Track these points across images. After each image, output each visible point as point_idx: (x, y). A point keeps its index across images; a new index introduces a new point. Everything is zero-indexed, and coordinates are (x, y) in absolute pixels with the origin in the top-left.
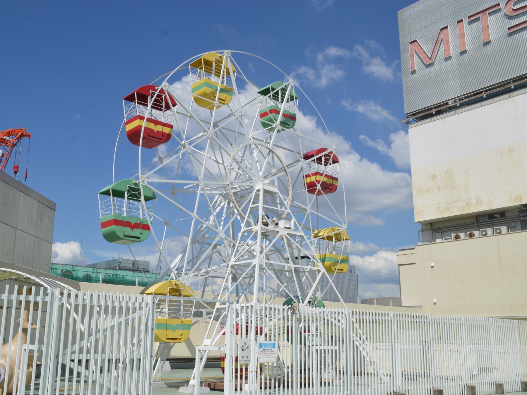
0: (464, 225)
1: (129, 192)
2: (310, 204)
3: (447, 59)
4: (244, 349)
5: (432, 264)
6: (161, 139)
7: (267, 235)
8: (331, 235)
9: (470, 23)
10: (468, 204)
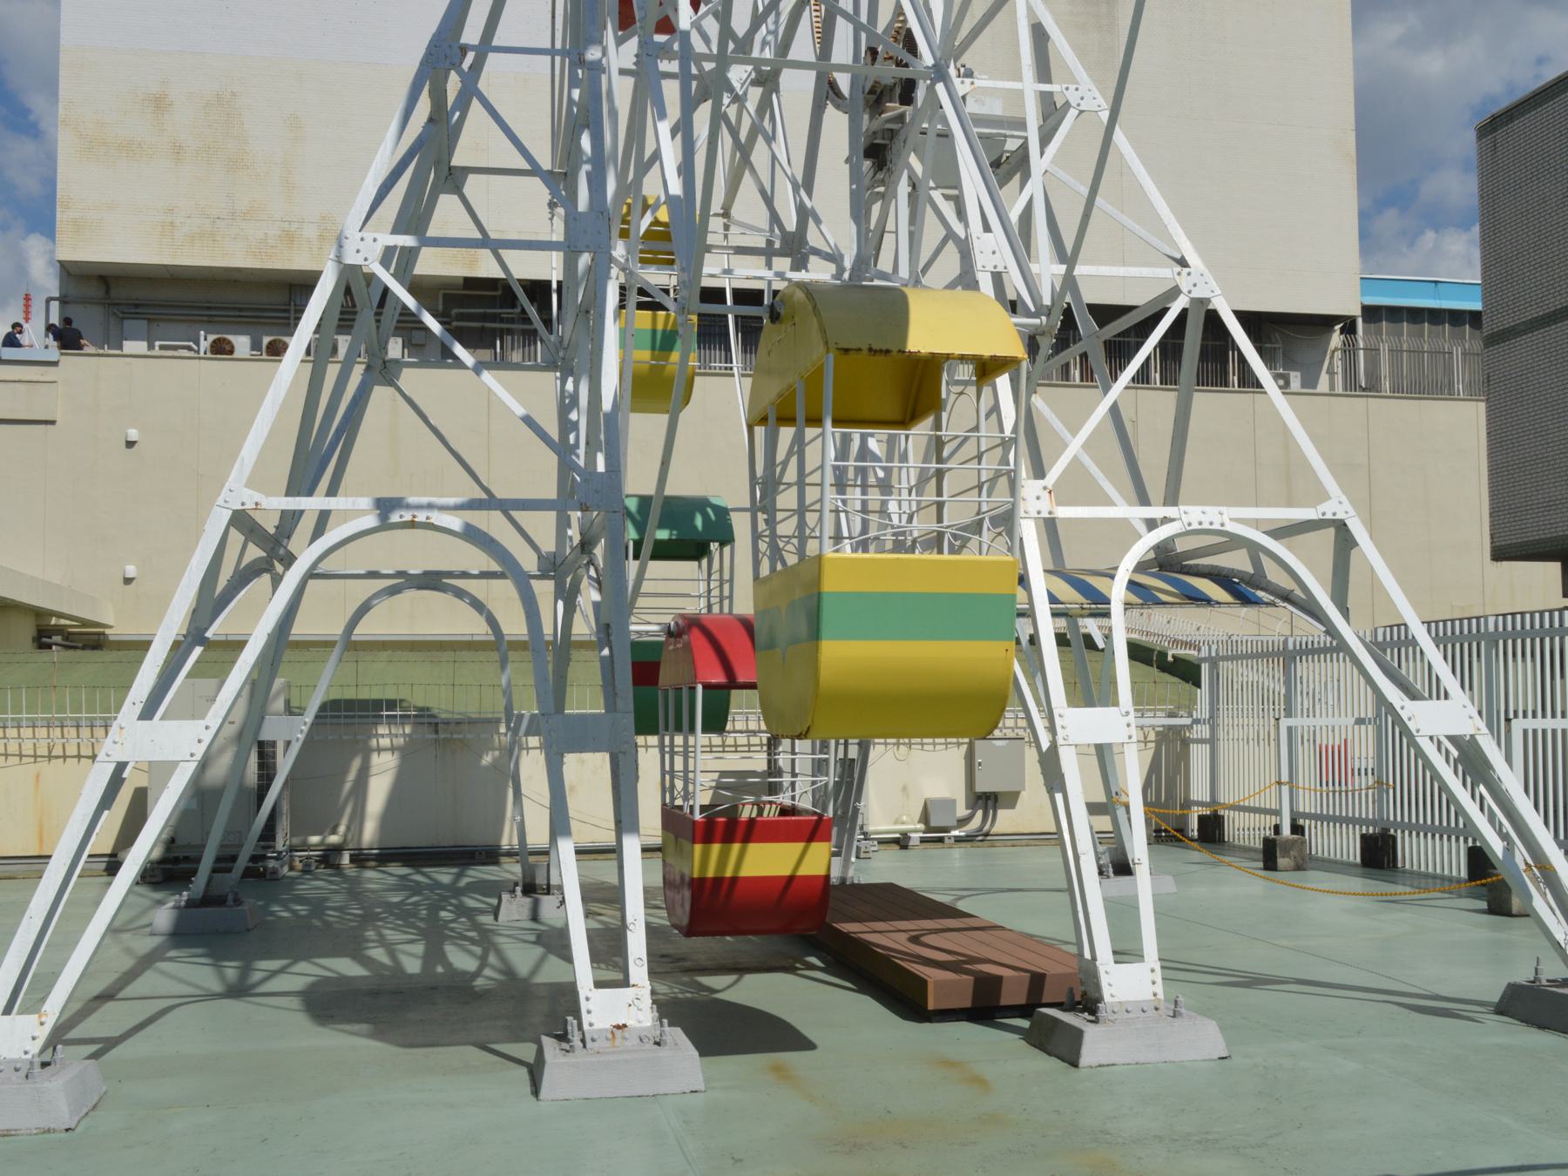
0: (241, 310)
5: (133, 434)
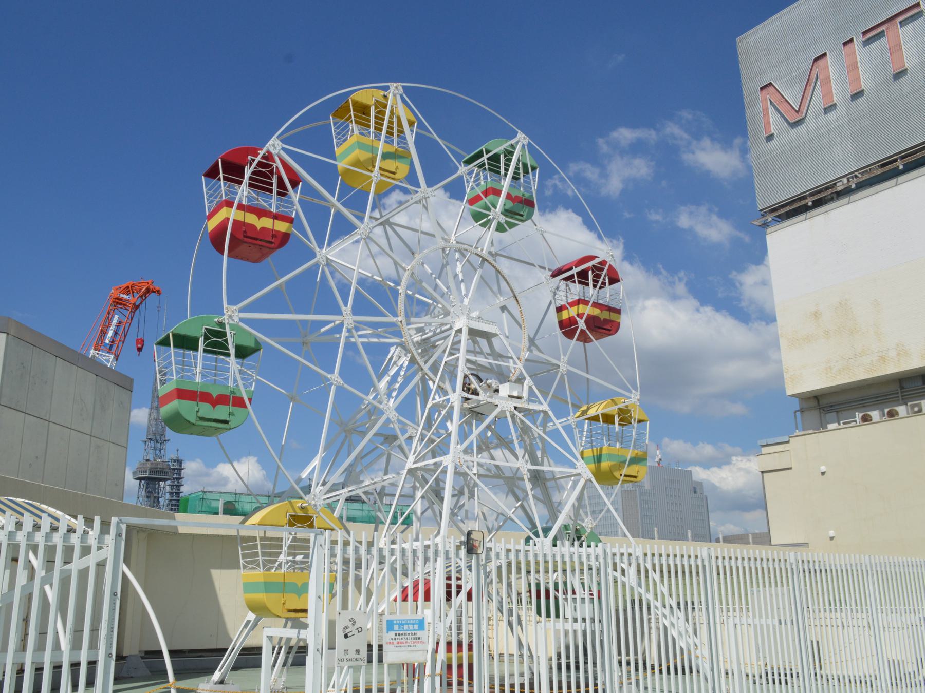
1: (206, 338)
2: (565, 355)
3: (827, 110)
4: (349, 635)
5: (823, 469)
6: (272, 243)
7: (479, 413)
8: (610, 413)
9: (867, 43)
10: (883, 359)
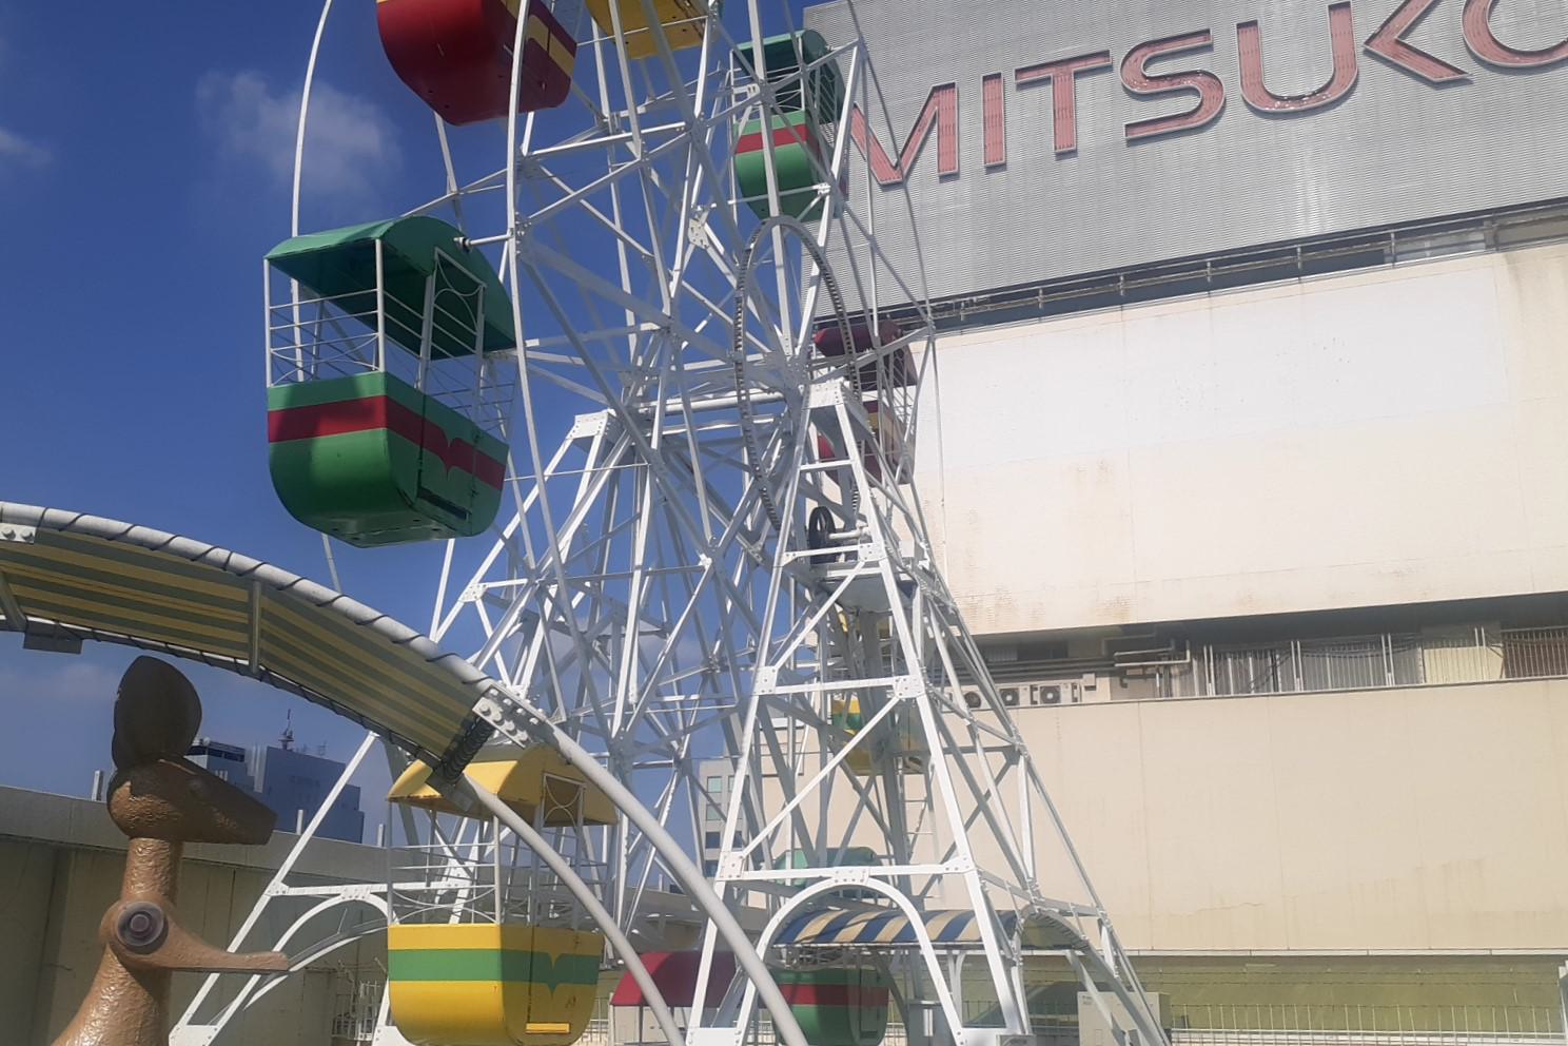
9: (1021, 86)
